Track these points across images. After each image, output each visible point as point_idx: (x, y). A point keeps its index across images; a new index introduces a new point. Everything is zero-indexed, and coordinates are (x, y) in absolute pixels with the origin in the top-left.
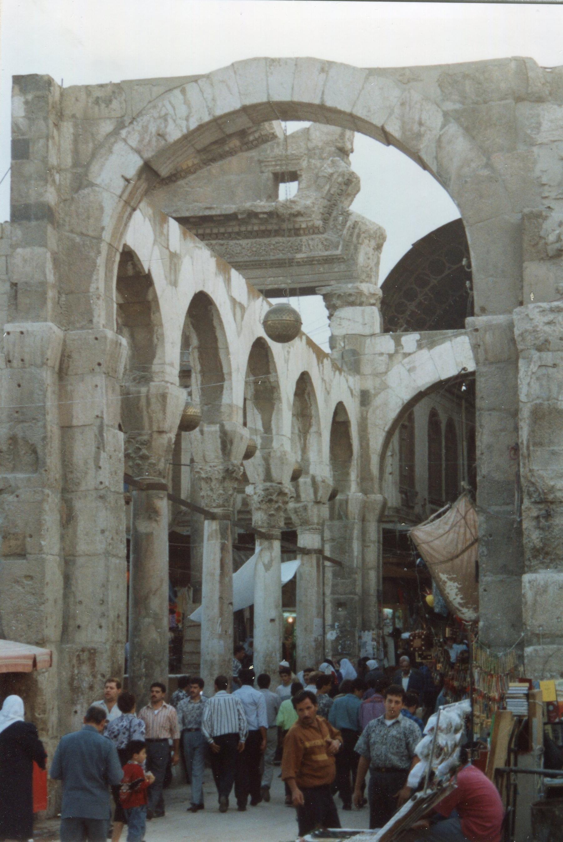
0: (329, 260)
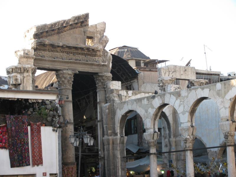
0: (103, 65)
